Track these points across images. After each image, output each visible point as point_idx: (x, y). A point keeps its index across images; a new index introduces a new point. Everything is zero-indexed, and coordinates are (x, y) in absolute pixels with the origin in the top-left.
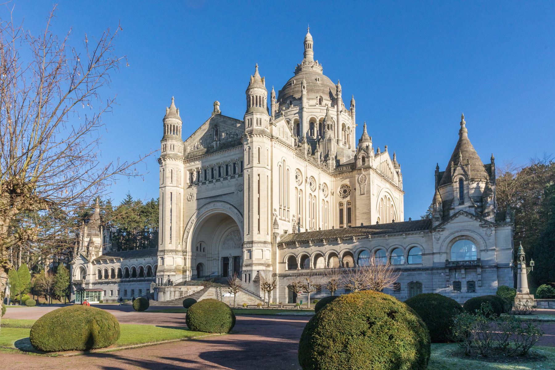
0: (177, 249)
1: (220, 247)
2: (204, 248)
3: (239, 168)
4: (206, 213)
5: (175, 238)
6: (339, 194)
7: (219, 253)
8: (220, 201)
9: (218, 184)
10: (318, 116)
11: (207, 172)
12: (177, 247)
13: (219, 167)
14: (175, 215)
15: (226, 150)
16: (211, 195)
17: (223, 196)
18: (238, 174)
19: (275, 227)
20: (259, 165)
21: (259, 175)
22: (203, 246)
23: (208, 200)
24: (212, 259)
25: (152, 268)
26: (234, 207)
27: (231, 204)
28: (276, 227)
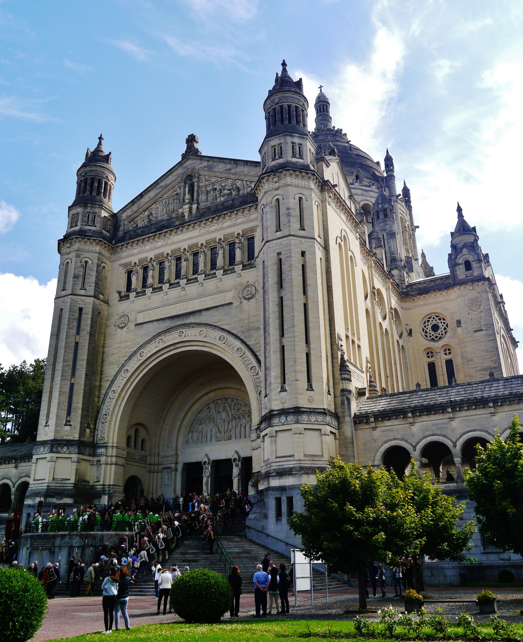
0: (82, 439)
1: (181, 439)
2: (143, 441)
3: (243, 252)
4: (158, 355)
5: (80, 411)
6: (423, 334)
7: (179, 453)
8: (195, 324)
9: (192, 289)
10: (359, 200)
11: (167, 264)
12: (82, 433)
13: (196, 255)
14: (86, 358)
15: (212, 218)
16: (174, 314)
17: (203, 313)
18: (242, 263)
19: (343, 376)
20: (302, 233)
21: (303, 254)
22: (143, 433)
23: (168, 324)
24: (160, 467)
25: (13, 490)
26: (233, 334)
27: (223, 330)
28: (346, 376)
